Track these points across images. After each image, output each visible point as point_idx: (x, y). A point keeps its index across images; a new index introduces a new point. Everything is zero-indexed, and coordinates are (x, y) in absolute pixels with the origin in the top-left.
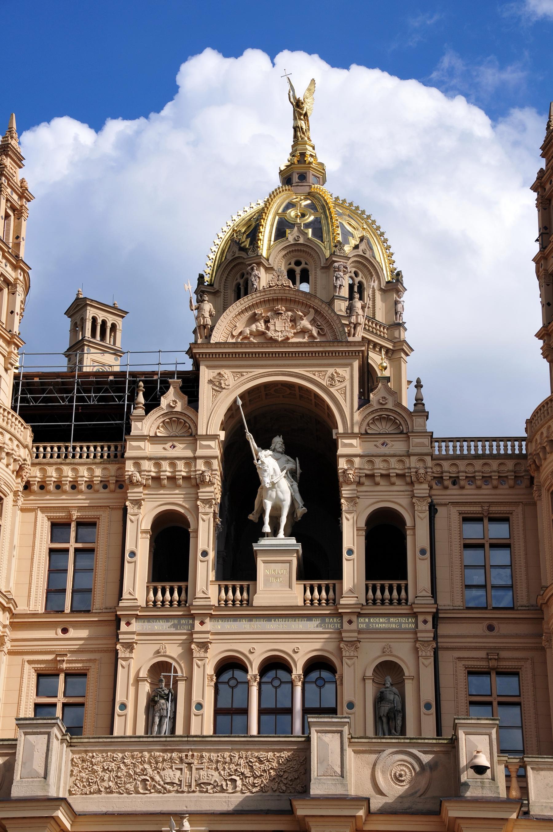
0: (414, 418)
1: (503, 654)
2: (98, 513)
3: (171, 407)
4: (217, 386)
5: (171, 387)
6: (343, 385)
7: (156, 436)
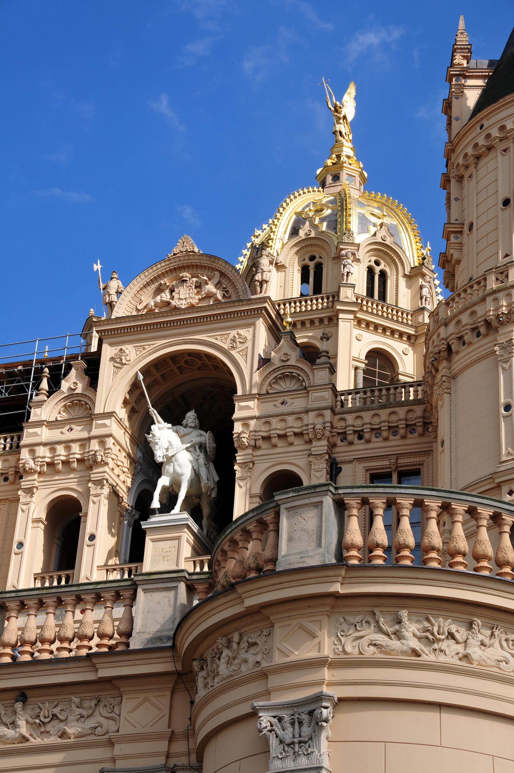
0: (315, 371)
3: (72, 389)
4: (118, 363)
5: (73, 369)
6: (245, 346)
7: (57, 420)
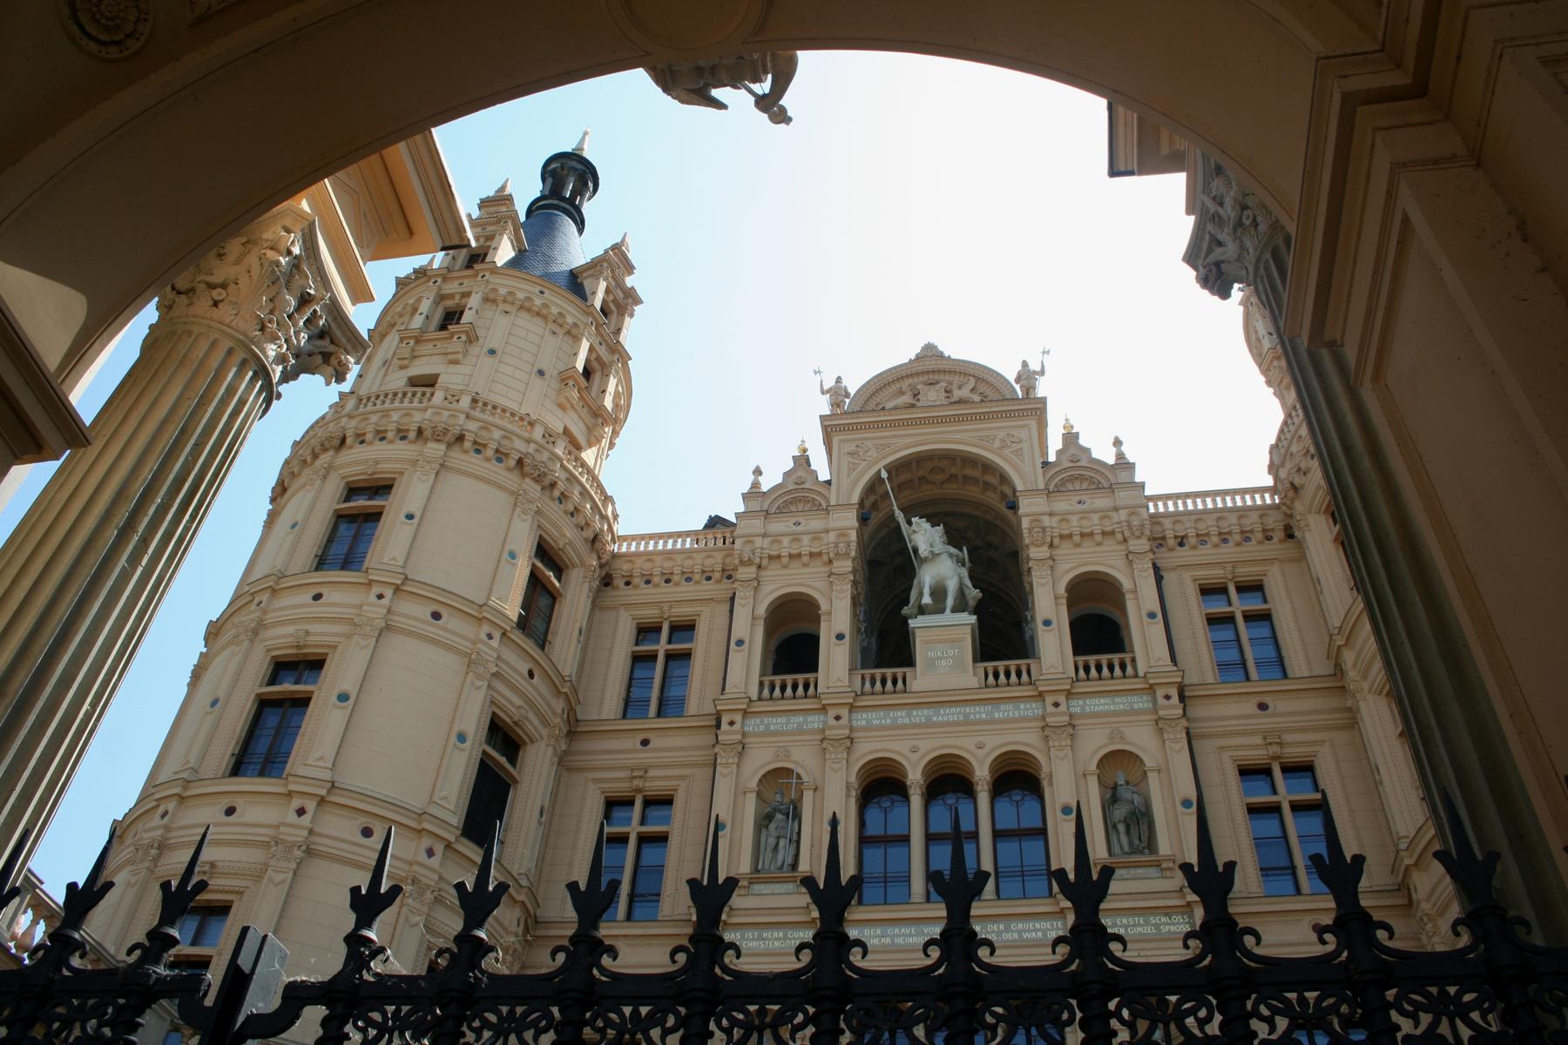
1: (1288, 738)
2: (699, 609)
